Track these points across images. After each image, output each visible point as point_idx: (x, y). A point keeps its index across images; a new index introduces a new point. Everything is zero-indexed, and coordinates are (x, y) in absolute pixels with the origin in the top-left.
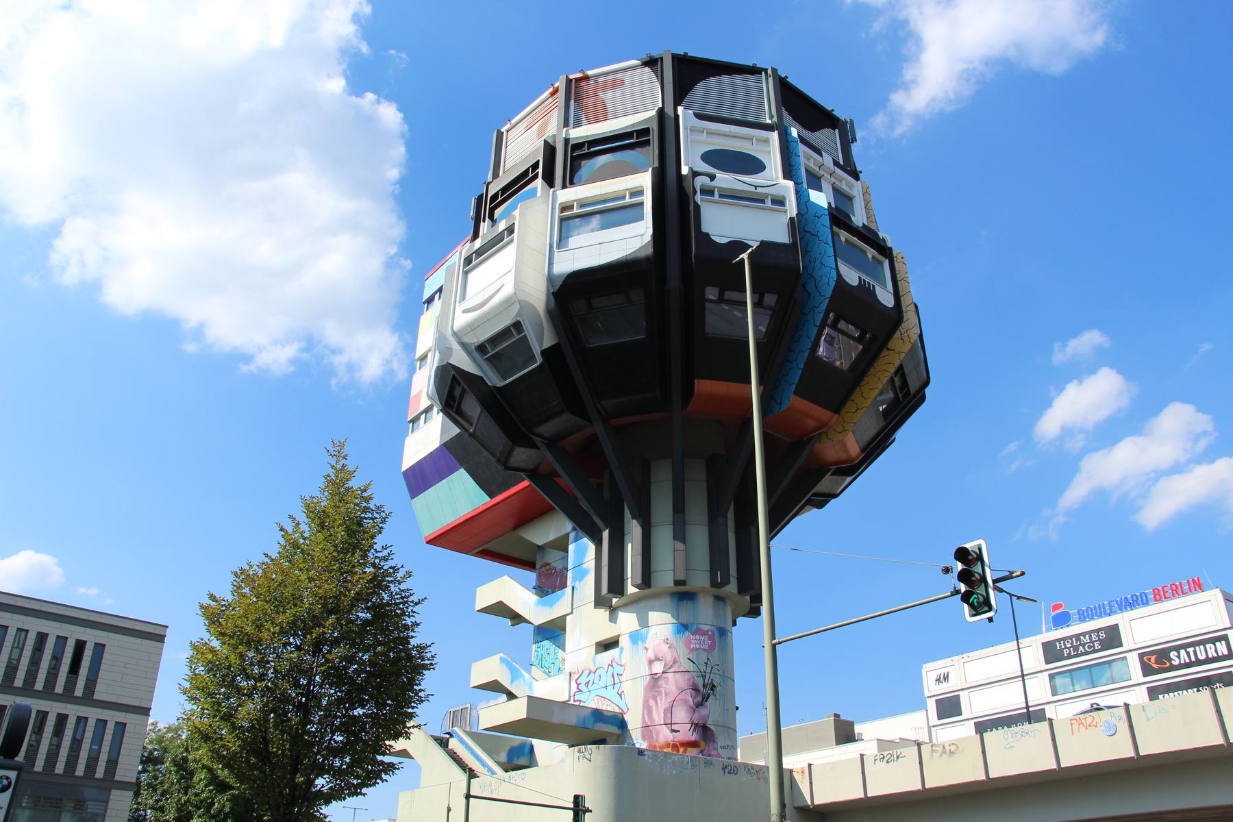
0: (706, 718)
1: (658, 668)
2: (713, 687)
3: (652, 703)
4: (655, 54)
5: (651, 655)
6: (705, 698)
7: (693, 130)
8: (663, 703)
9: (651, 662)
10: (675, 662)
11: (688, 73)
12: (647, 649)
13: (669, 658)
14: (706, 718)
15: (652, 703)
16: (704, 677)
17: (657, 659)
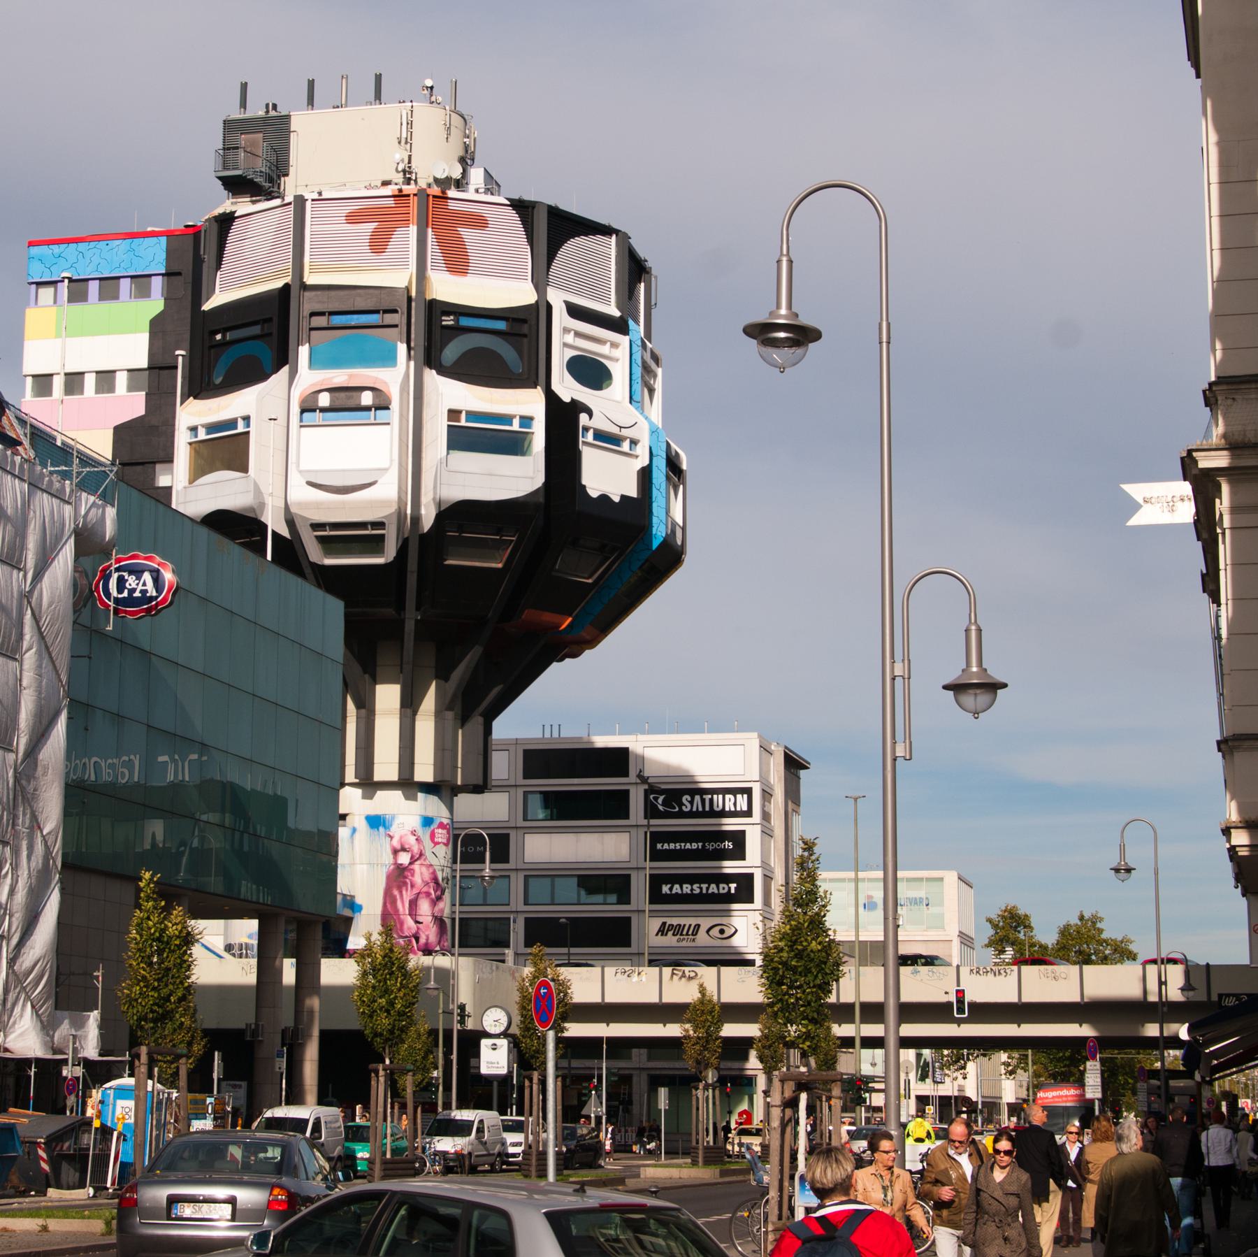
0: (442, 911)
1: (404, 859)
3: (396, 893)
4: (529, 196)
5: (396, 843)
7: (566, 330)
8: (408, 895)
9: (395, 852)
10: (421, 855)
11: (553, 229)
12: (391, 837)
13: (416, 849)
14: (442, 911)
15: (396, 893)
17: (403, 849)
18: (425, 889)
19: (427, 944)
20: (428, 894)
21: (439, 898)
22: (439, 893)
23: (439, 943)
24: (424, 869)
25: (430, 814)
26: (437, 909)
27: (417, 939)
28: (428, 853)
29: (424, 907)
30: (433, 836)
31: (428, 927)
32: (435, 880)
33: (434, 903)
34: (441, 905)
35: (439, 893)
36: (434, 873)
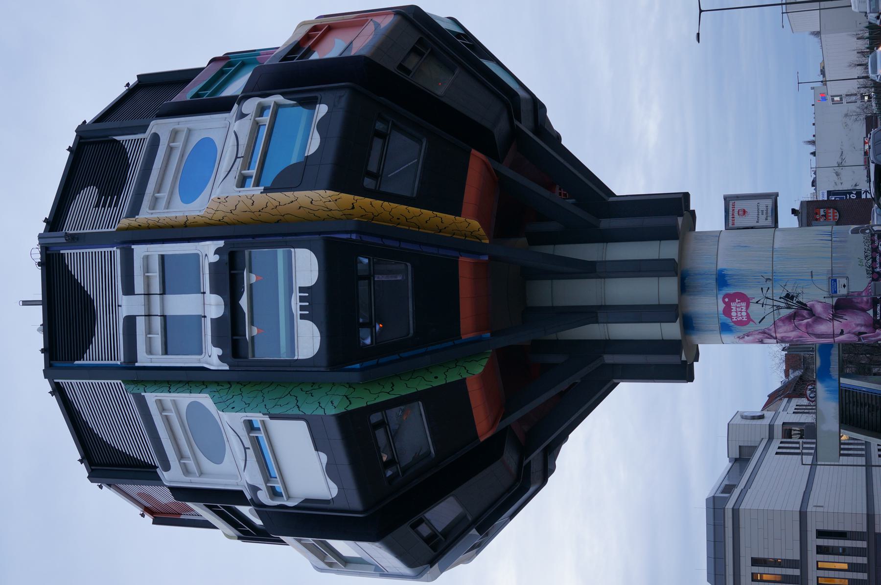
0: (825, 306)
2: (789, 297)
6: (803, 306)
14: (825, 306)
16: (779, 308)
18: (803, 329)
19: (865, 325)
20: (808, 326)
21: (811, 312)
22: (805, 313)
23: (864, 310)
24: (780, 330)
25: (717, 327)
26: (824, 316)
27: (860, 333)
28: (763, 326)
29: (823, 328)
30: (741, 323)
31: (846, 325)
32: (790, 318)
33: (818, 319)
34: (819, 309)
35: (805, 313)
36: (780, 319)
